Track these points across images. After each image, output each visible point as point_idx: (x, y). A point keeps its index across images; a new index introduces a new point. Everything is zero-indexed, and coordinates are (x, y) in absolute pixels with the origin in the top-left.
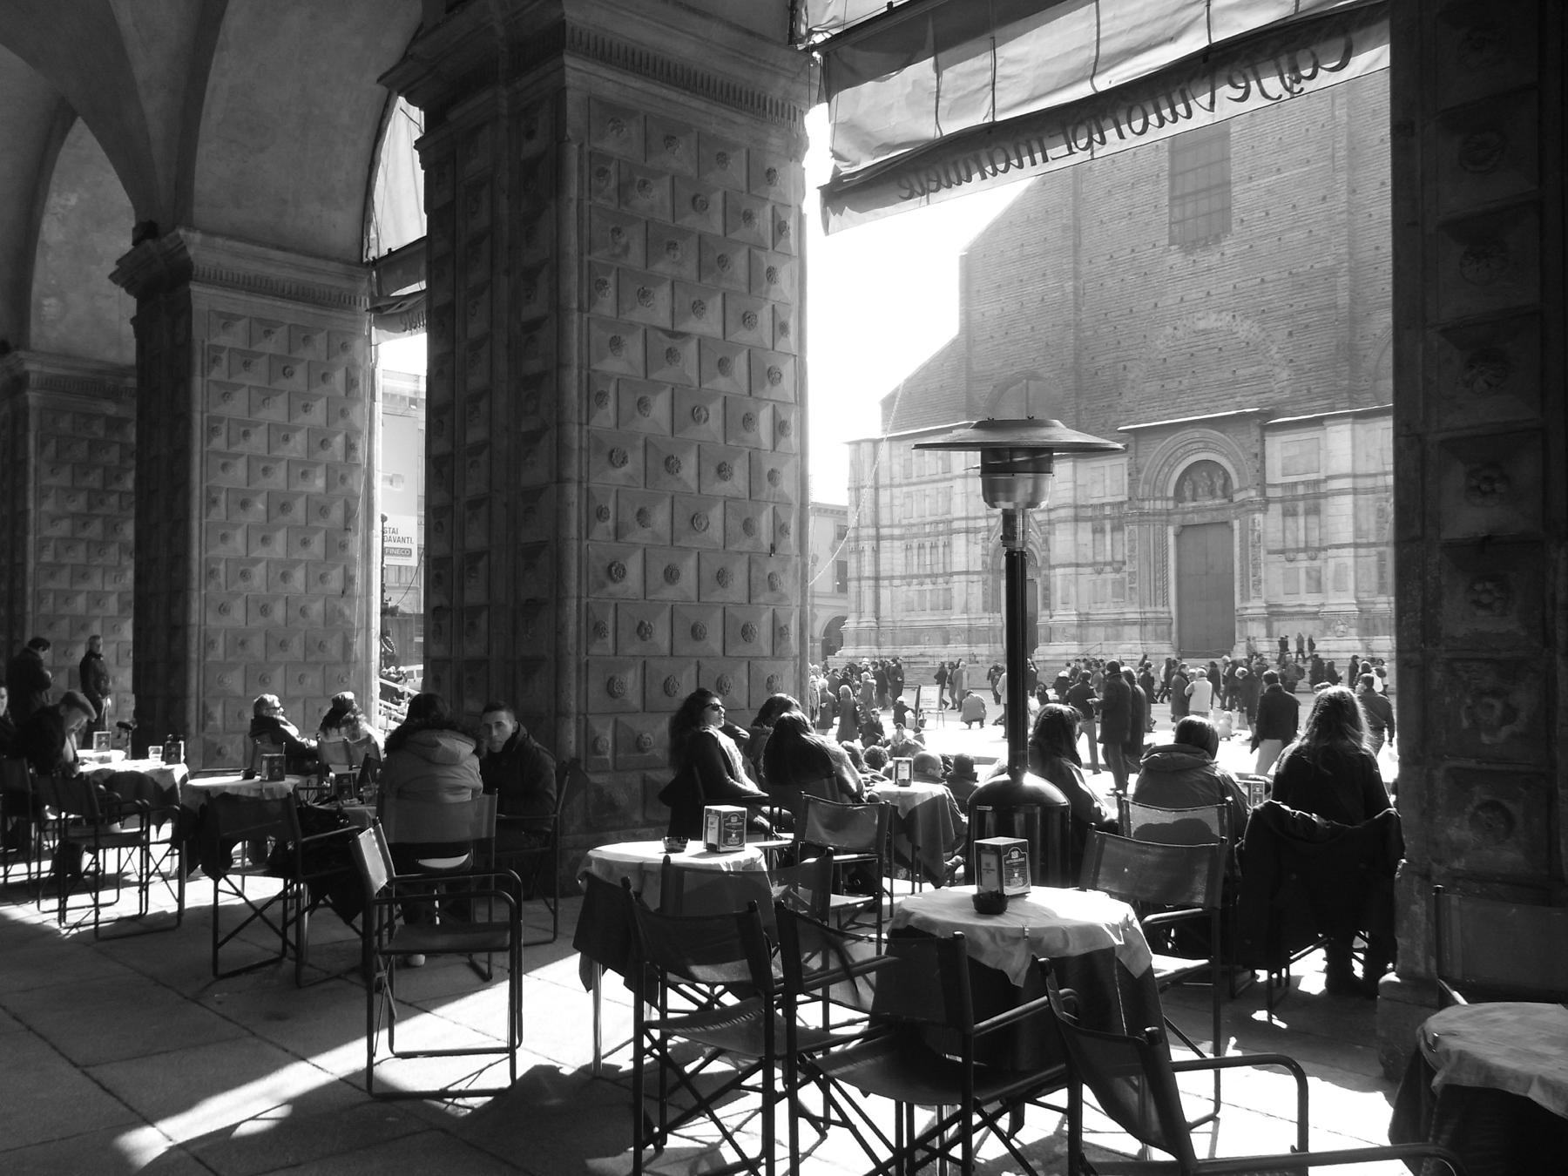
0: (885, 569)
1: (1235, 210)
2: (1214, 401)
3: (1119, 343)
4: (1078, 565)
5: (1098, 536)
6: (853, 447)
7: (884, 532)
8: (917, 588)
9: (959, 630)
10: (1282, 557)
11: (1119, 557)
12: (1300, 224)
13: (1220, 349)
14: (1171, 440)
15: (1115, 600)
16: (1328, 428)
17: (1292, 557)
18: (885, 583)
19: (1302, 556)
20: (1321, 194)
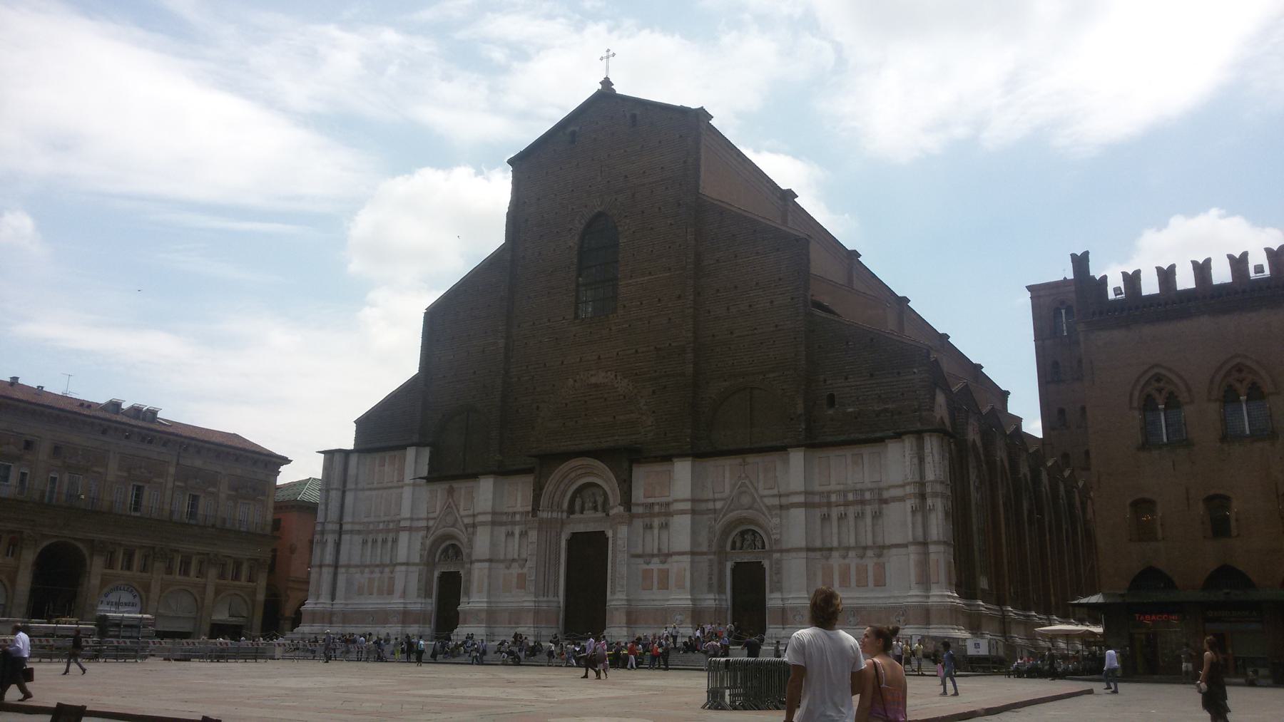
0: (343, 559)
3: (535, 389)
4: (490, 561)
7: (346, 527)
10: (641, 561)
11: (524, 556)
13: (605, 399)
14: (565, 467)
15: (517, 590)
16: (675, 464)
18: (342, 570)
19: (656, 560)
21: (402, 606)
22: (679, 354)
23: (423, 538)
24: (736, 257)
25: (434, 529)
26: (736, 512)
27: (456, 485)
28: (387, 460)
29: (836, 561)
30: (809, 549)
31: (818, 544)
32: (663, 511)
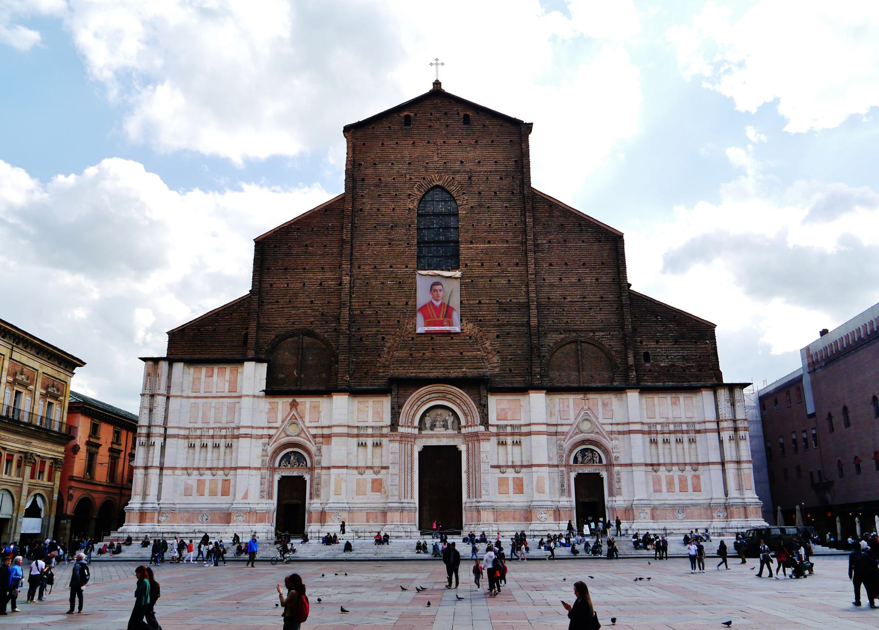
1: (462, 257)
2: (448, 369)
3: (379, 322)
4: (347, 467)
5: (361, 449)
6: (150, 363)
7: (169, 432)
9: (239, 511)
10: (498, 470)
12: (502, 275)
17: (504, 471)
18: (165, 472)
19: (511, 470)
21: (247, 506)
22: (519, 309)
23: (264, 445)
24: (565, 241)
25: (276, 437)
26: (581, 435)
27: (298, 400)
28: (216, 370)
29: (663, 472)
30: (646, 465)
31: (649, 462)
32: (516, 431)
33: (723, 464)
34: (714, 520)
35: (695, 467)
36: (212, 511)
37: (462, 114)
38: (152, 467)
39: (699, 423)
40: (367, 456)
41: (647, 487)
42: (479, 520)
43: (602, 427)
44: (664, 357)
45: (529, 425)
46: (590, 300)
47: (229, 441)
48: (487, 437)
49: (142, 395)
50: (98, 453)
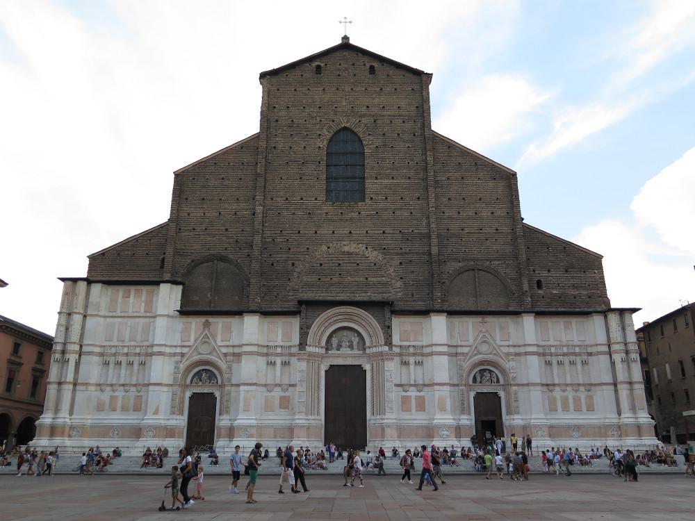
1: (367, 191)
3: (289, 249)
6: (69, 283)
7: (85, 349)
8: (111, 393)
10: (400, 389)
13: (358, 264)
18: (78, 387)
20: (417, 195)
23: (177, 362)
24: (462, 178)
26: (480, 356)
27: (212, 320)
28: (133, 292)
29: (558, 394)
30: (543, 385)
31: (544, 382)
33: (615, 385)
34: (608, 438)
35: (588, 387)
36: (122, 427)
37: (368, 65)
38: (65, 382)
39: (591, 346)
40: (275, 373)
41: (544, 405)
42: (383, 436)
43: (499, 349)
44: (556, 285)
45: (431, 345)
46: (486, 231)
47: (142, 358)
48: (391, 357)
49: (60, 313)
50: (19, 371)
